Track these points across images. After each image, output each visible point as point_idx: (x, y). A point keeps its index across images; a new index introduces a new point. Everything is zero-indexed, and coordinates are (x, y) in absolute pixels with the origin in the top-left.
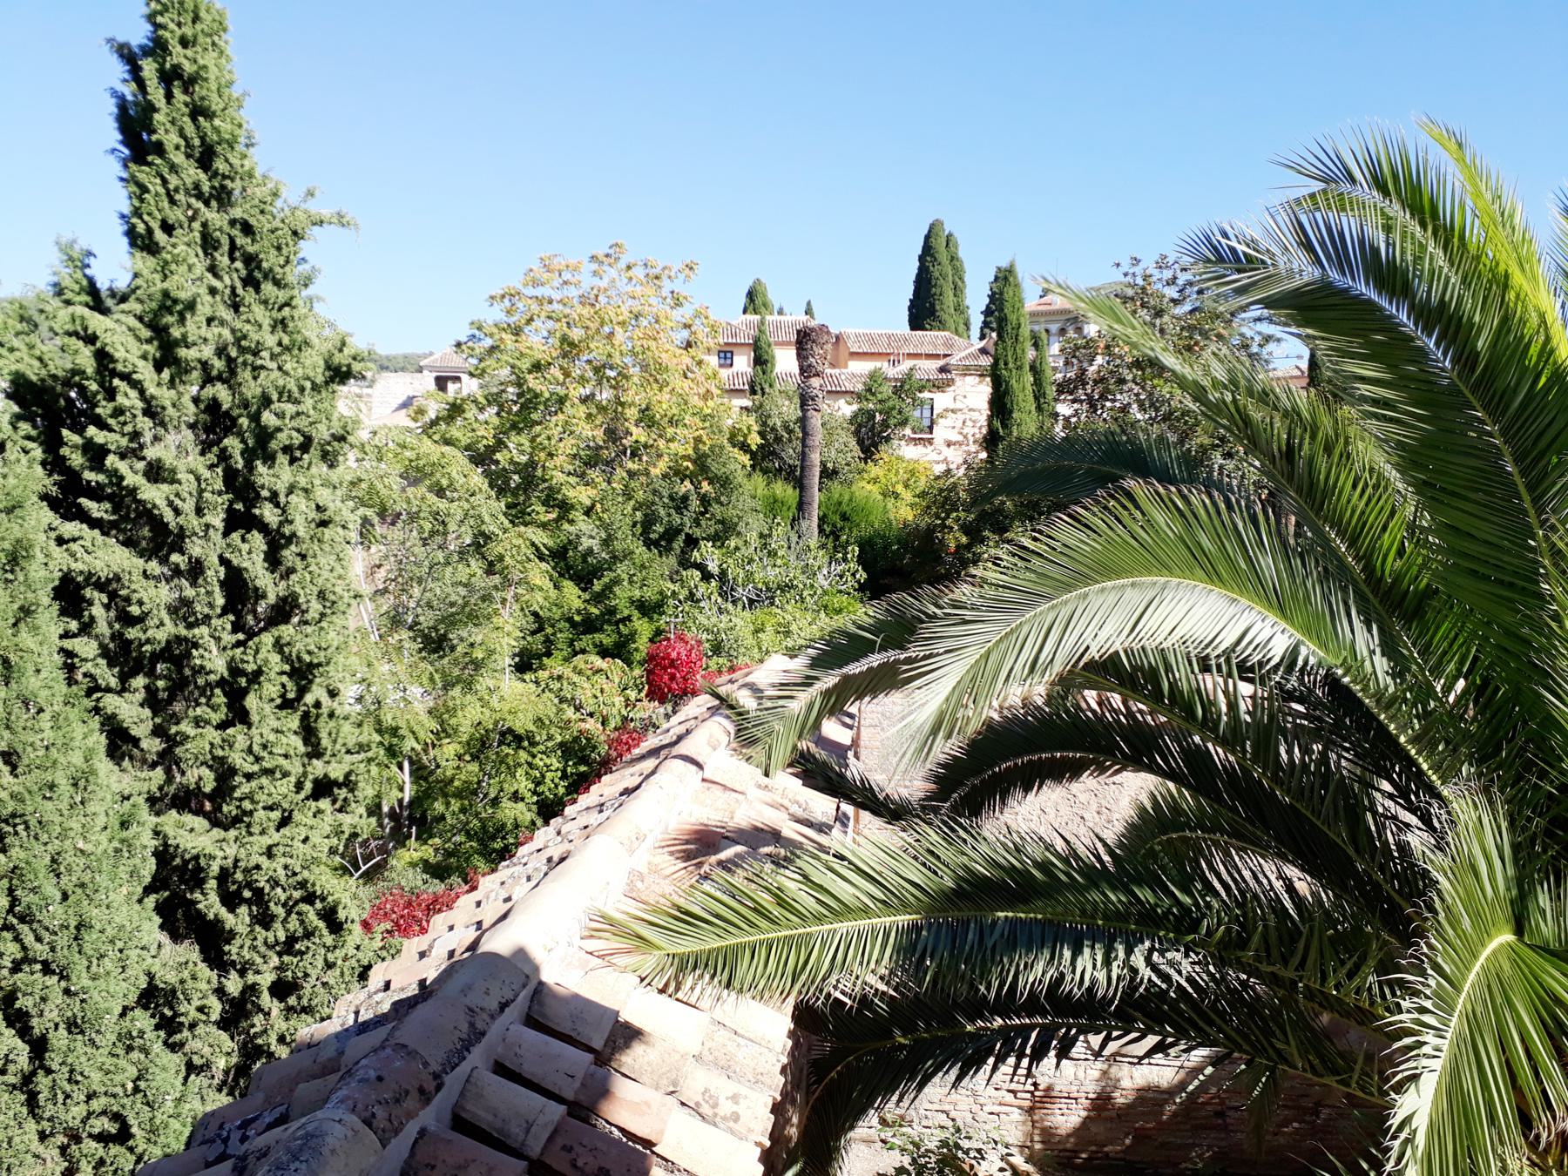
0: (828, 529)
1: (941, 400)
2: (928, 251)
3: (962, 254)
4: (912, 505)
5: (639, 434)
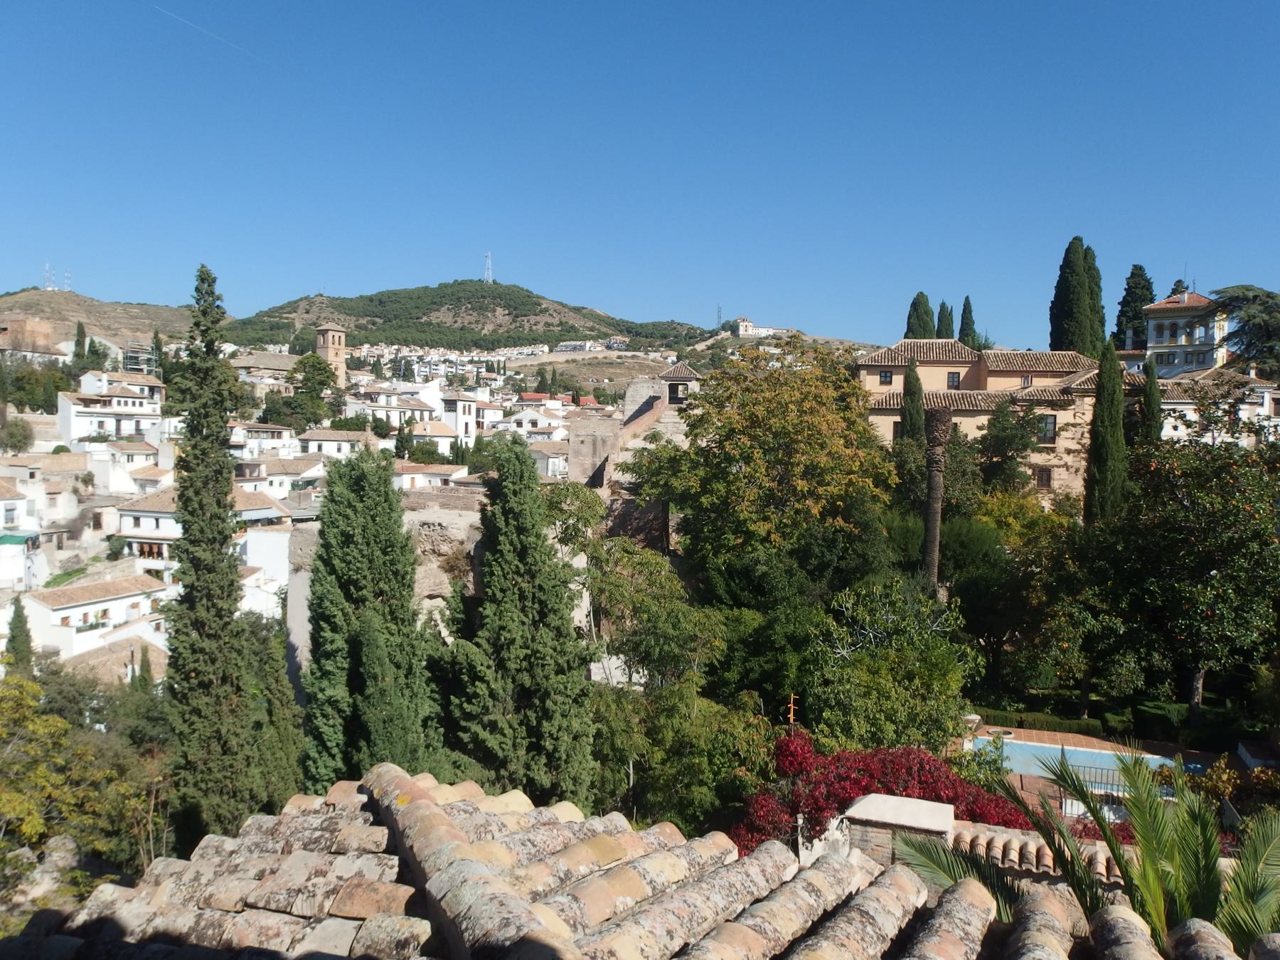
0: (949, 554)
1: (1063, 417)
2: (1067, 266)
3: (1098, 264)
4: (1021, 535)
5: (802, 485)
